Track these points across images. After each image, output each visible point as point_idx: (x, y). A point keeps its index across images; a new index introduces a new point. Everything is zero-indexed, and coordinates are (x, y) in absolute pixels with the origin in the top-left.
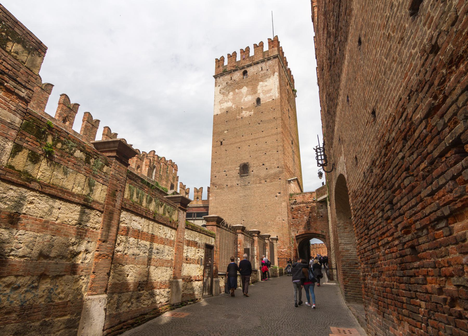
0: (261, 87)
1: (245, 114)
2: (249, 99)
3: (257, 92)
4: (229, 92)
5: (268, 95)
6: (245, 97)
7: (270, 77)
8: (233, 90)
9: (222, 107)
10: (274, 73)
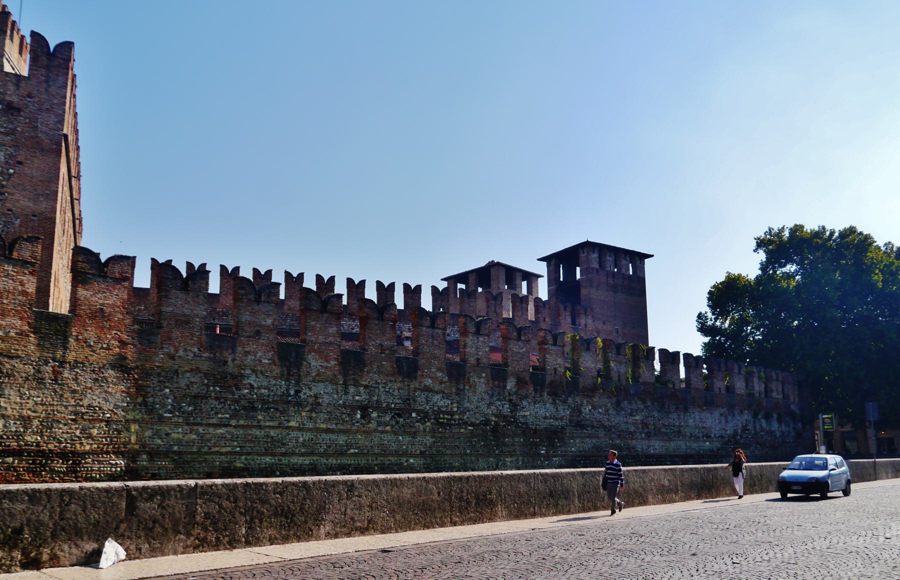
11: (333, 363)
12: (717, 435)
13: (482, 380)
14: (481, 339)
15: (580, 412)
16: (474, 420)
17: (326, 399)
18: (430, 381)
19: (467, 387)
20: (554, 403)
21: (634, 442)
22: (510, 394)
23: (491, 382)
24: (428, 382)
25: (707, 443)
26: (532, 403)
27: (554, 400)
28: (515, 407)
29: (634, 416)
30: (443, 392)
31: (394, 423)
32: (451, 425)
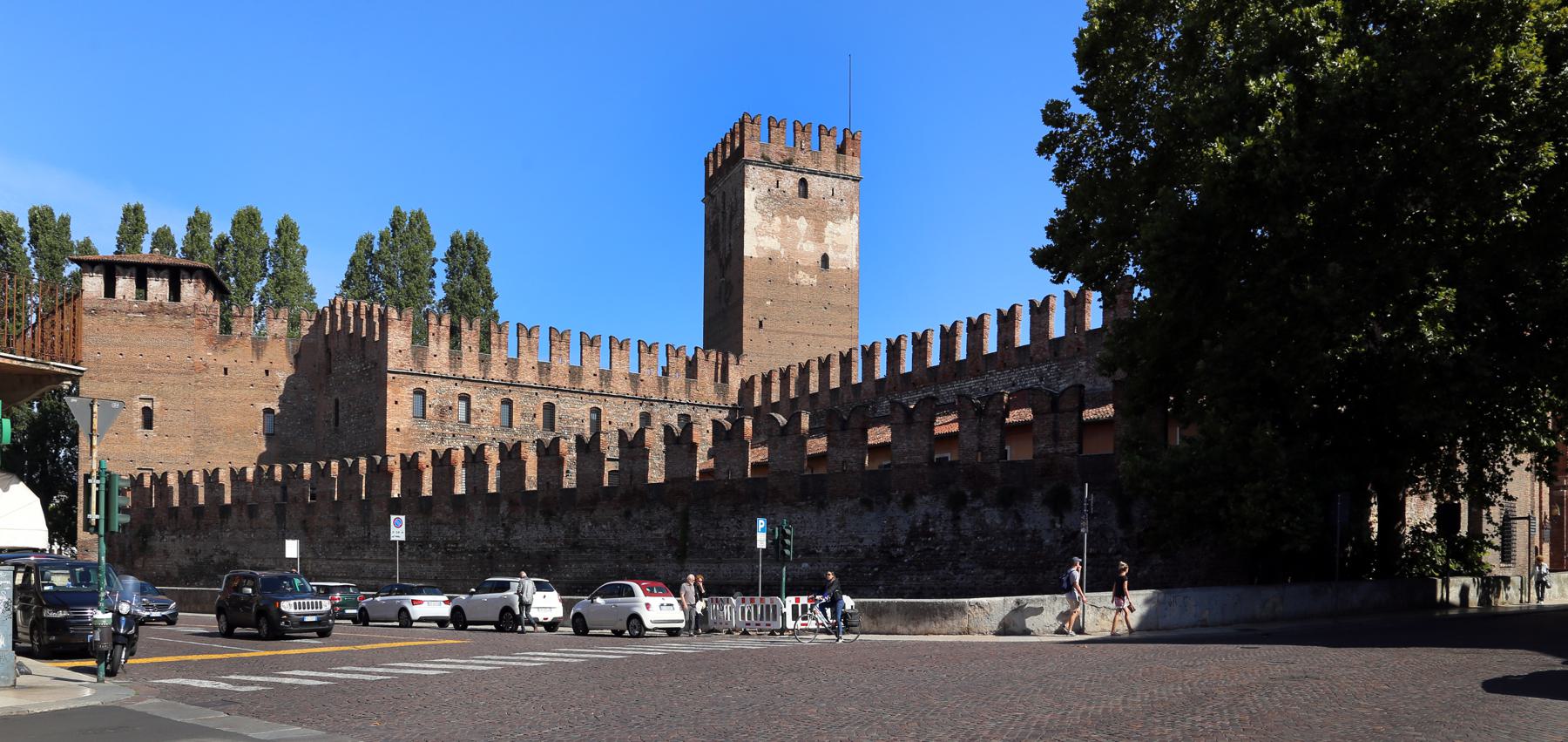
0: (830, 232)
1: (804, 278)
2: (809, 250)
3: (823, 241)
4: (773, 216)
5: (841, 256)
6: (804, 242)
7: (845, 218)
8: (782, 214)
9: (762, 244)
10: (852, 213)
11: (385, 509)
12: (833, 550)
13: (479, 508)
14: (477, 467)
15: (578, 531)
16: (472, 548)
17: (380, 539)
18: (441, 515)
19: (467, 517)
20: (547, 523)
21: (653, 565)
22: (502, 519)
23: (486, 508)
24: (439, 516)
25: (805, 565)
26: (524, 526)
27: (547, 520)
28: (508, 531)
29: (655, 529)
30: (449, 524)
31: (418, 553)
32: (455, 553)
